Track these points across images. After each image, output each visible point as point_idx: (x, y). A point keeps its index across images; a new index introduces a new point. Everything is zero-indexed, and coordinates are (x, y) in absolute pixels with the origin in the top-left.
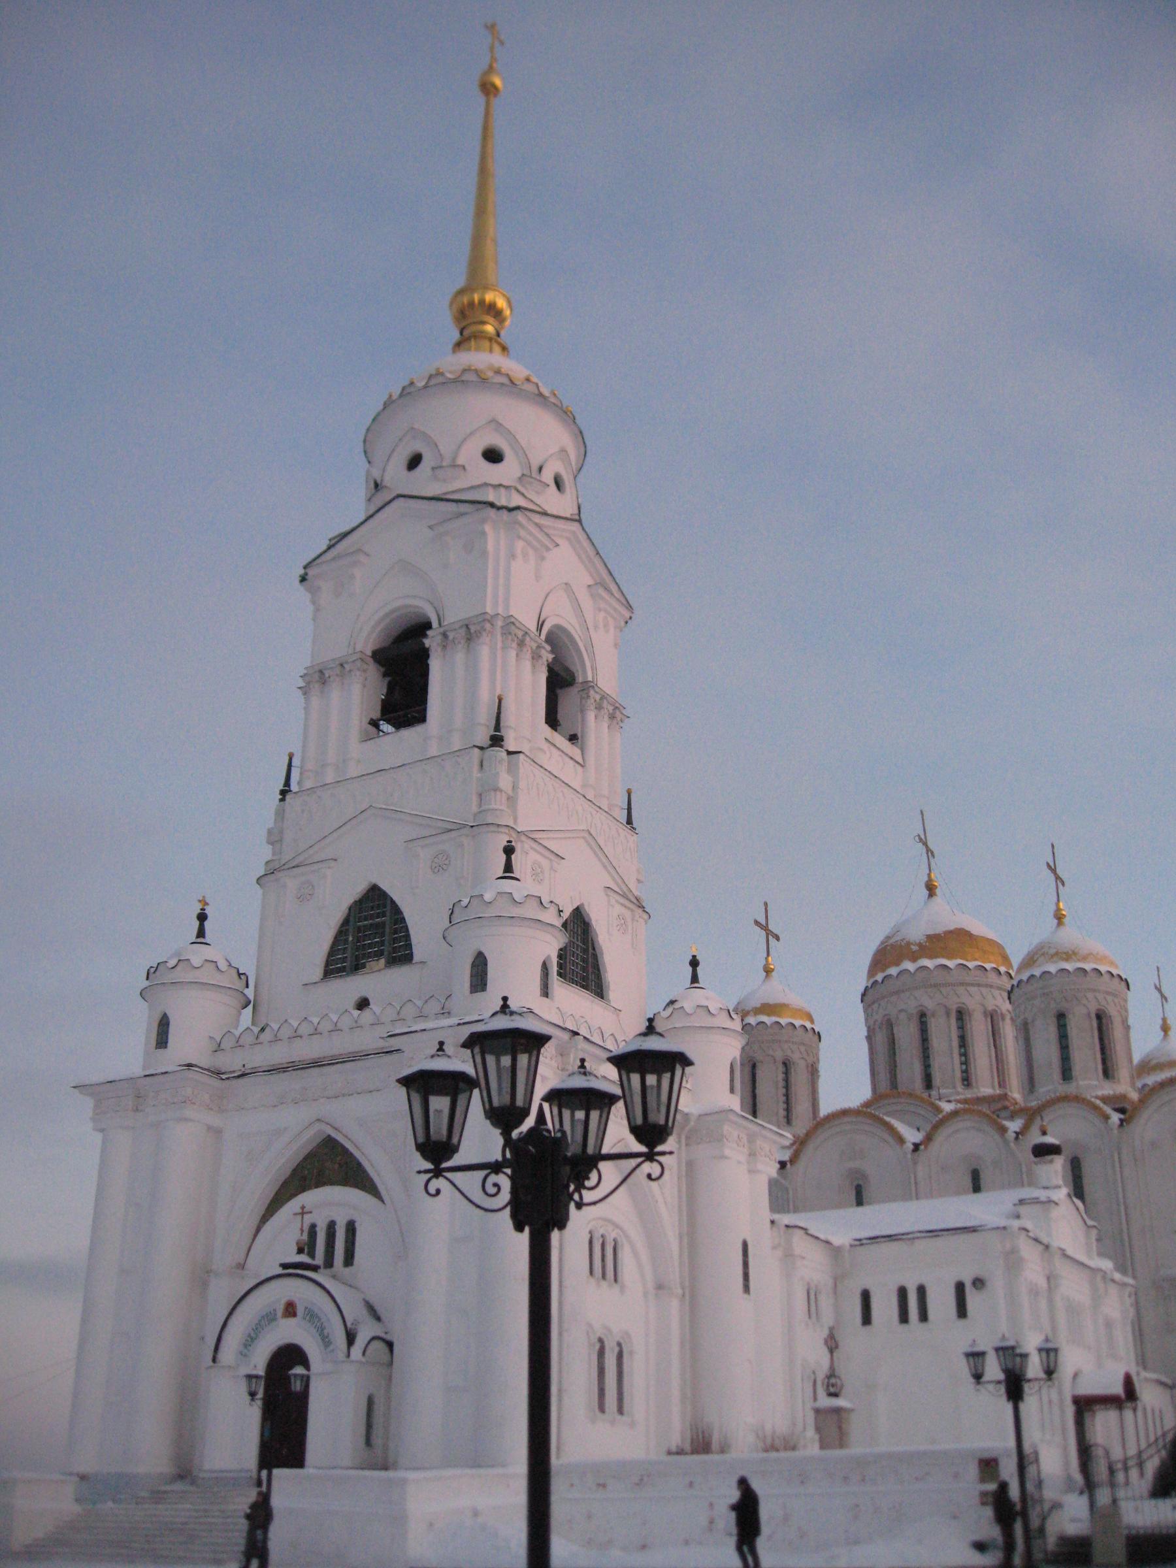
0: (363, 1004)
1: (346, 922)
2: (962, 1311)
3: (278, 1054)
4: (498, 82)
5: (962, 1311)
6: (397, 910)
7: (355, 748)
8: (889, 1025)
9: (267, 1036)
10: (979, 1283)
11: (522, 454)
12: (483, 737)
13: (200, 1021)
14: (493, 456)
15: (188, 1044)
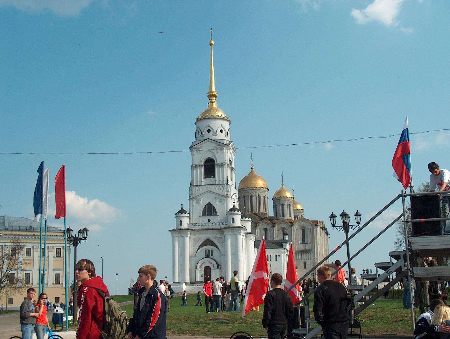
0: (209, 220)
1: (205, 207)
2: (276, 260)
3: (200, 228)
4: (213, 43)
5: (276, 260)
6: (214, 207)
7: (203, 180)
8: (245, 197)
9: (197, 225)
10: (279, 256)
11: (225, 131)
12: (225, 182)
13: (186, 222)
14: (221, 131)
15: (185, 225)
